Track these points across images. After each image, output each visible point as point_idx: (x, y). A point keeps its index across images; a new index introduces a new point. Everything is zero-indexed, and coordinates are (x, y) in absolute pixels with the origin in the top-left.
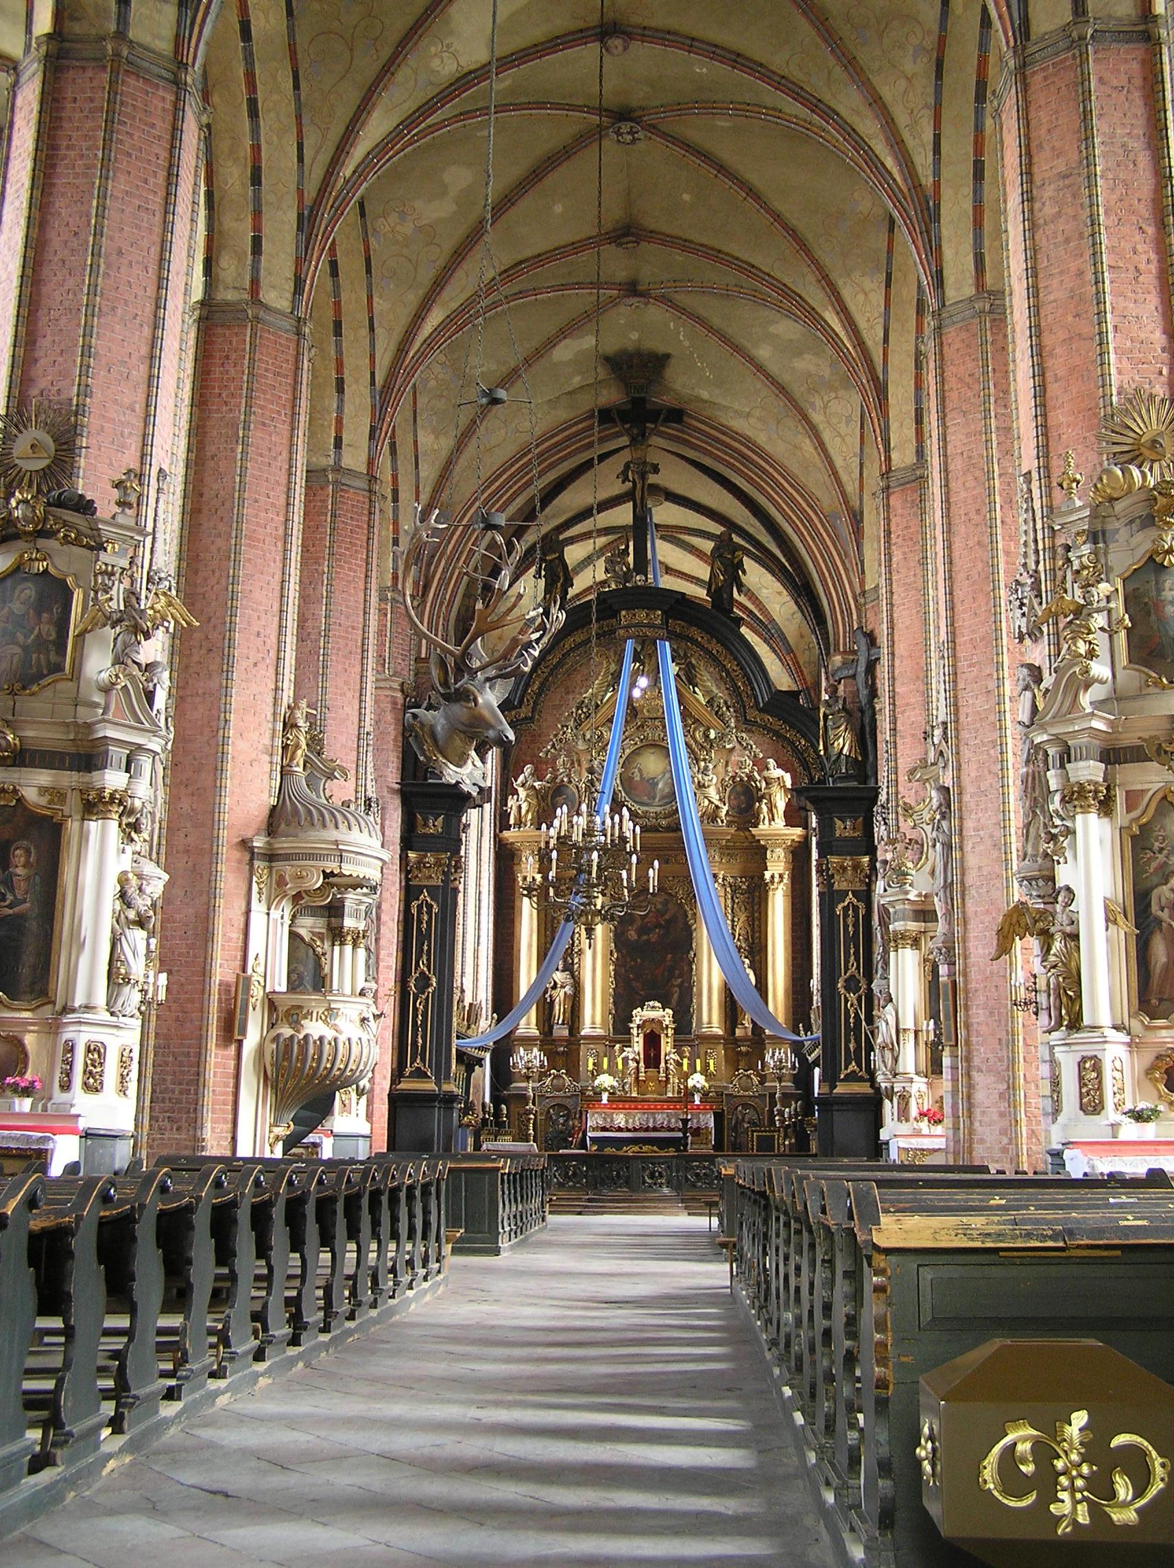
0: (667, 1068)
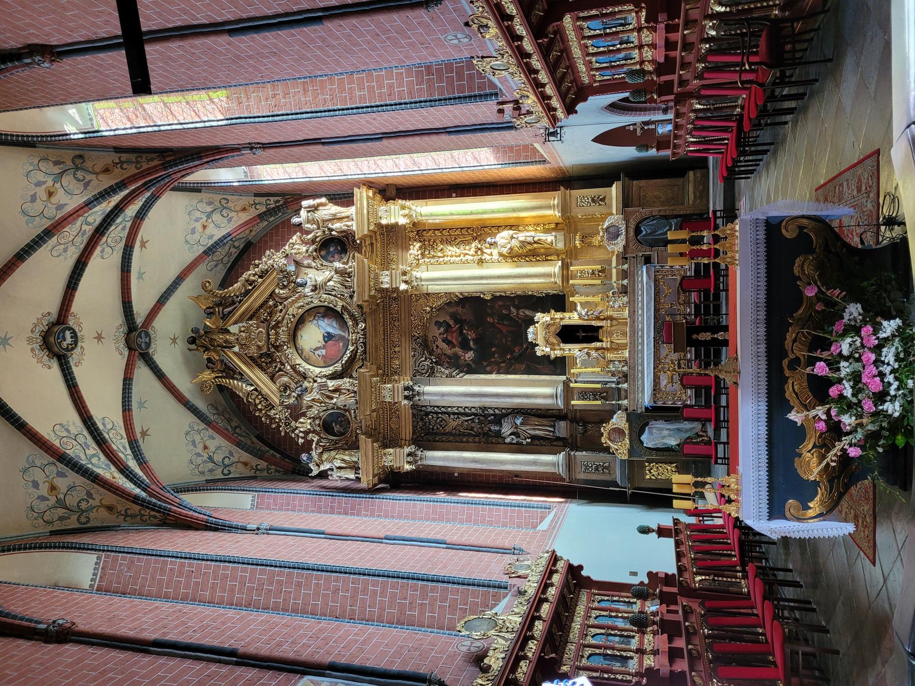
0: (598, 318)
